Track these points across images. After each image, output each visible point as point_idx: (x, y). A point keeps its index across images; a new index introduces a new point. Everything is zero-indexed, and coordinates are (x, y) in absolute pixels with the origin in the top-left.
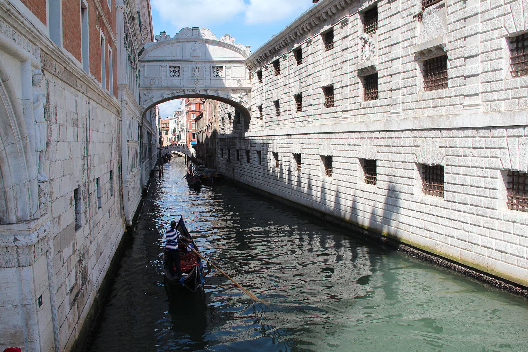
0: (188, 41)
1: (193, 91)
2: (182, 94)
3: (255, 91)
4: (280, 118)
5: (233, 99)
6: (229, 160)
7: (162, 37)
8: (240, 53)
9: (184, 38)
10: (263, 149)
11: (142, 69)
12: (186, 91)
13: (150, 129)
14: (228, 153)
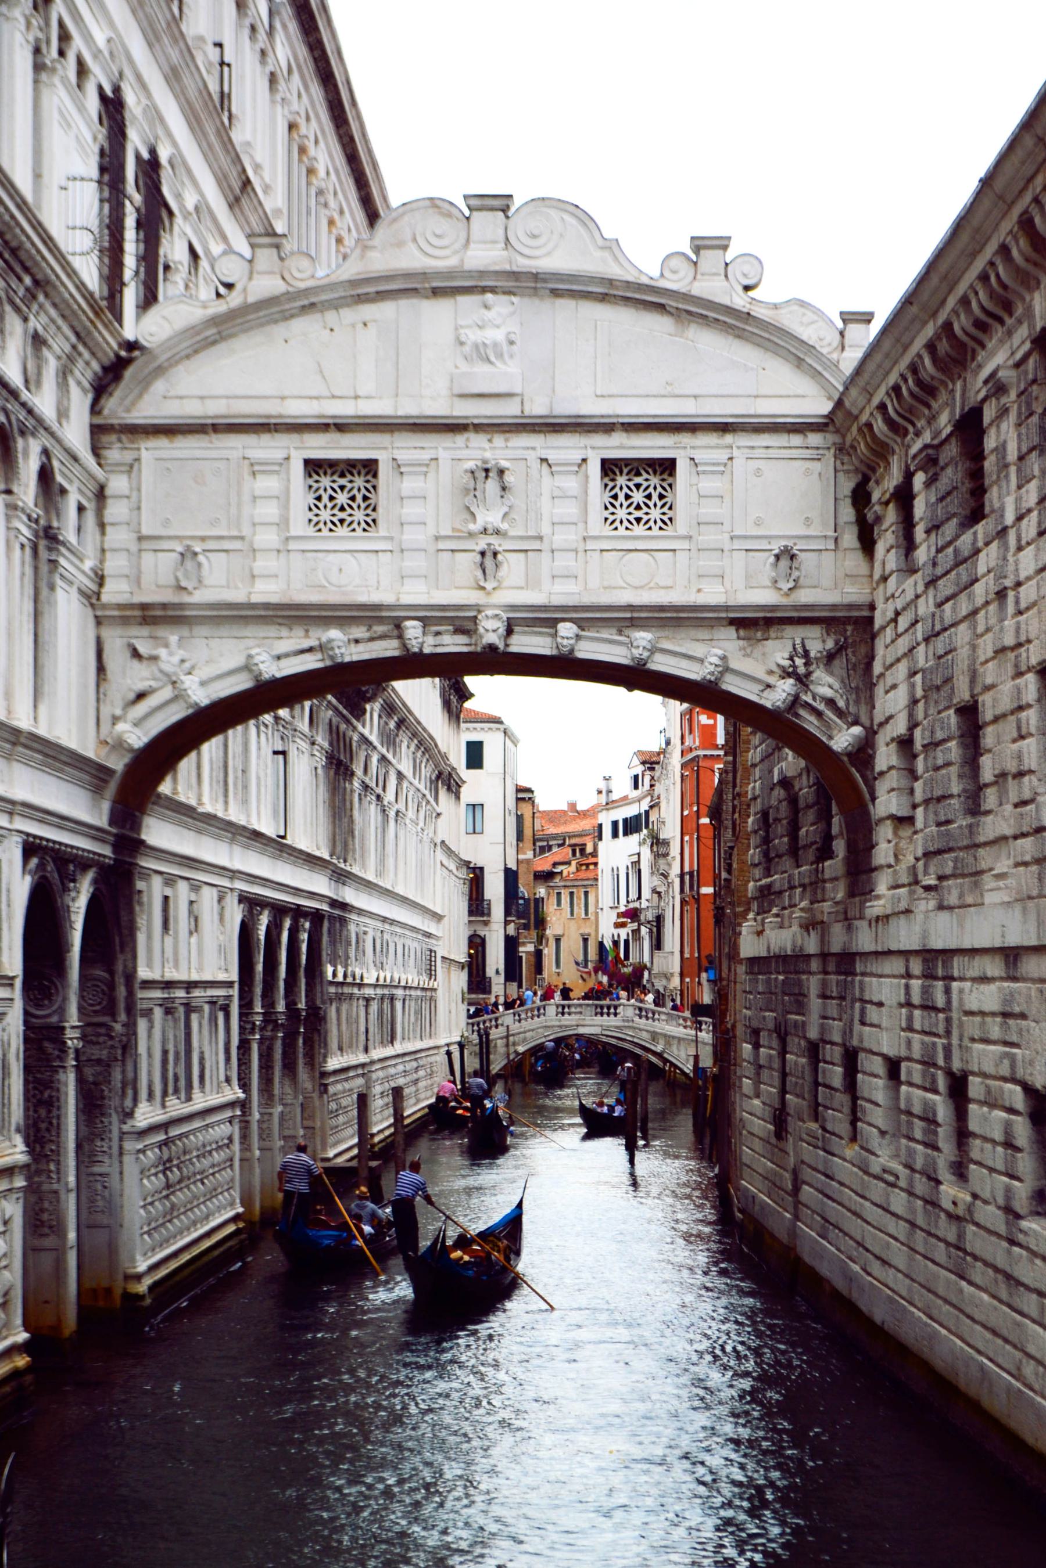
0: (437, 292)
1: (459, 631)
2: (388, 649)
3: (889, 632)
4: (992, 827)
5: (748, 691)
6: (780, 1119)
7: (261, 264)
8: (799, 363)
9: (408, 275)
10: (909, 1042)
11: (118, 484)
12: (413, 630)
13: (320, 884)
14: (776, 1065)
